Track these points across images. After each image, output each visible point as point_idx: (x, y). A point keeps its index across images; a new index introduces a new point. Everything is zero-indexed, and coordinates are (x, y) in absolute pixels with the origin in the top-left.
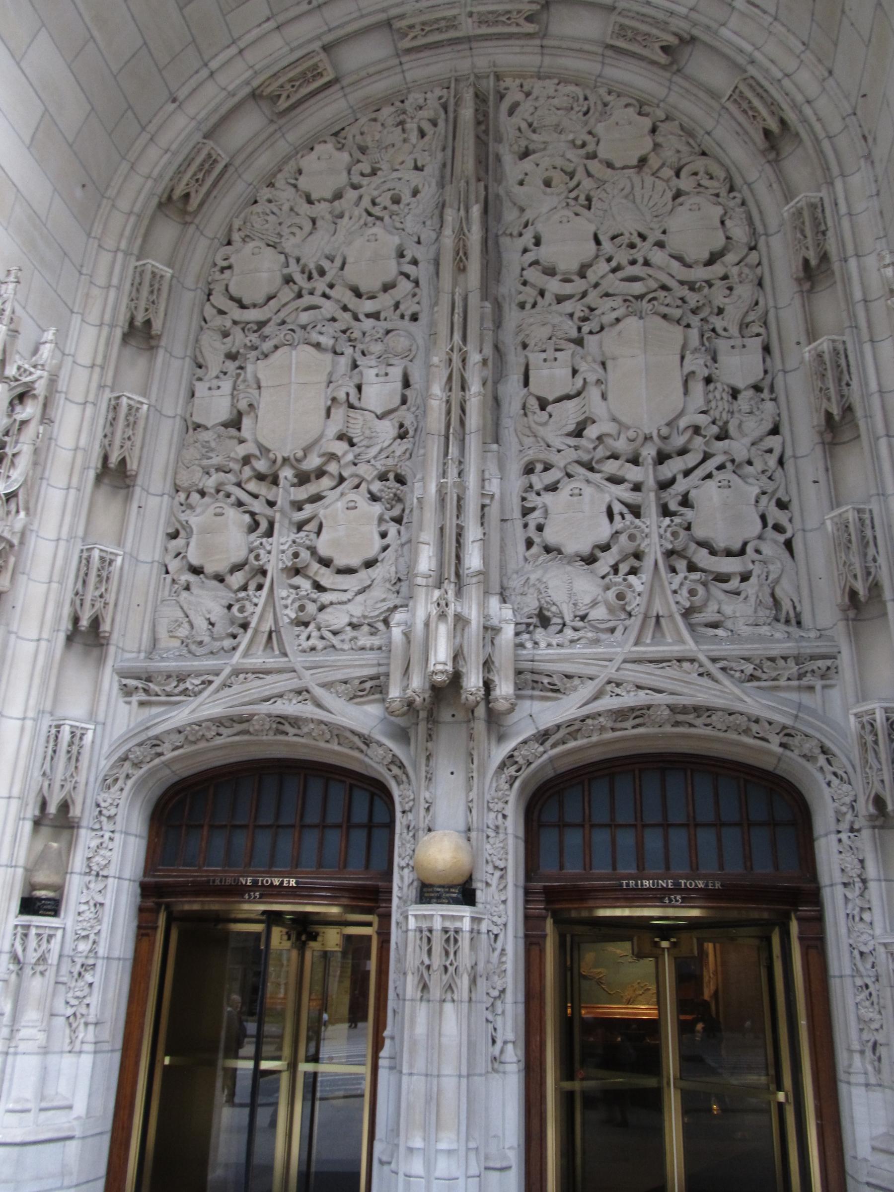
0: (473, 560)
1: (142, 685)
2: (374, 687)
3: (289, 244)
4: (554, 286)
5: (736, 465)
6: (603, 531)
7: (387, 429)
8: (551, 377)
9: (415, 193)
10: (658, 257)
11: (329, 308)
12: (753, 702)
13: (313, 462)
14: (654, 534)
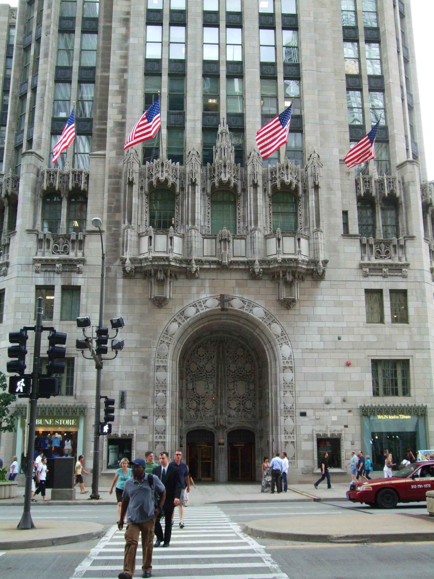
0: (224, 412)
1: (187, 422)
2: (213, 423)
3: (198, 363)
4: (231, 374)
5: (250, 399)
6: (236, 406)
7: (212, 392)
8: (231, 386)
9: (214, 356)
10: (244, 371)
11: (203, 374)
12: (250, 426)
13: (203, 396)
14: (242, 407)
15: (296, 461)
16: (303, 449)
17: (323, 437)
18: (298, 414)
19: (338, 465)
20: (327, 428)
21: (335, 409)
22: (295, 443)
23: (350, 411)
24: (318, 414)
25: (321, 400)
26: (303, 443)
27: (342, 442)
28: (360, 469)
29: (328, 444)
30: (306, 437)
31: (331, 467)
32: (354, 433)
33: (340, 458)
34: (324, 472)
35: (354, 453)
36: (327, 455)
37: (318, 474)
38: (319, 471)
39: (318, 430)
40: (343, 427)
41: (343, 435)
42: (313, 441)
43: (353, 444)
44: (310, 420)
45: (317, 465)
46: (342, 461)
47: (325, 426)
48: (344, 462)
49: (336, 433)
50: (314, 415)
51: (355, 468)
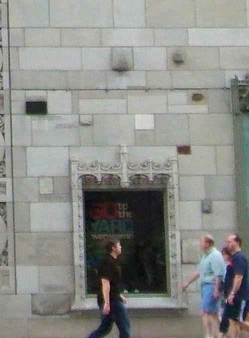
15: (10, 268)
16: (35, 226)
17: (104, 187)
18: (18, 107)
19: (159, 285)
20: (119, 155)
21: (147, 90)
22: (9, 208)
23: (197, 98)
24: (87, 106)
25: (96, 60)
26: (37, 208)
27: (169, 203)
28: (231, 297)
29: (123, 212)
30: (46, 188)
31: (131, 290)
32: (212, 171)
33: (164, 258)
34: (107, 306)
35: (210, 243)
36: (119, 247)
37: (86, 314)
38: (91, 303)
39: (89, 162)
40: (173, 152)
41: (174, 181)
42: (70, 200)
43: (207, 211)
44: (58, 126)
45: (83, 282)
46: (171, 270)
47: (114, 149)
48: (178, 274)
49: (151, 173)
50: (75, 110)
51: (216, 293)
